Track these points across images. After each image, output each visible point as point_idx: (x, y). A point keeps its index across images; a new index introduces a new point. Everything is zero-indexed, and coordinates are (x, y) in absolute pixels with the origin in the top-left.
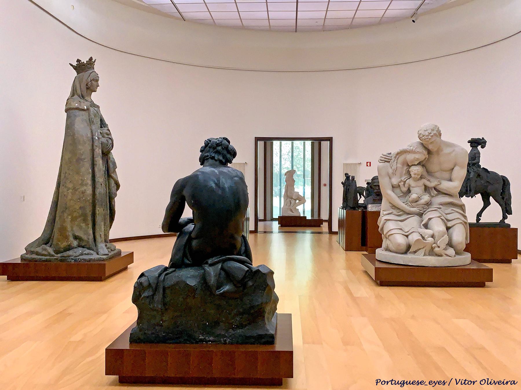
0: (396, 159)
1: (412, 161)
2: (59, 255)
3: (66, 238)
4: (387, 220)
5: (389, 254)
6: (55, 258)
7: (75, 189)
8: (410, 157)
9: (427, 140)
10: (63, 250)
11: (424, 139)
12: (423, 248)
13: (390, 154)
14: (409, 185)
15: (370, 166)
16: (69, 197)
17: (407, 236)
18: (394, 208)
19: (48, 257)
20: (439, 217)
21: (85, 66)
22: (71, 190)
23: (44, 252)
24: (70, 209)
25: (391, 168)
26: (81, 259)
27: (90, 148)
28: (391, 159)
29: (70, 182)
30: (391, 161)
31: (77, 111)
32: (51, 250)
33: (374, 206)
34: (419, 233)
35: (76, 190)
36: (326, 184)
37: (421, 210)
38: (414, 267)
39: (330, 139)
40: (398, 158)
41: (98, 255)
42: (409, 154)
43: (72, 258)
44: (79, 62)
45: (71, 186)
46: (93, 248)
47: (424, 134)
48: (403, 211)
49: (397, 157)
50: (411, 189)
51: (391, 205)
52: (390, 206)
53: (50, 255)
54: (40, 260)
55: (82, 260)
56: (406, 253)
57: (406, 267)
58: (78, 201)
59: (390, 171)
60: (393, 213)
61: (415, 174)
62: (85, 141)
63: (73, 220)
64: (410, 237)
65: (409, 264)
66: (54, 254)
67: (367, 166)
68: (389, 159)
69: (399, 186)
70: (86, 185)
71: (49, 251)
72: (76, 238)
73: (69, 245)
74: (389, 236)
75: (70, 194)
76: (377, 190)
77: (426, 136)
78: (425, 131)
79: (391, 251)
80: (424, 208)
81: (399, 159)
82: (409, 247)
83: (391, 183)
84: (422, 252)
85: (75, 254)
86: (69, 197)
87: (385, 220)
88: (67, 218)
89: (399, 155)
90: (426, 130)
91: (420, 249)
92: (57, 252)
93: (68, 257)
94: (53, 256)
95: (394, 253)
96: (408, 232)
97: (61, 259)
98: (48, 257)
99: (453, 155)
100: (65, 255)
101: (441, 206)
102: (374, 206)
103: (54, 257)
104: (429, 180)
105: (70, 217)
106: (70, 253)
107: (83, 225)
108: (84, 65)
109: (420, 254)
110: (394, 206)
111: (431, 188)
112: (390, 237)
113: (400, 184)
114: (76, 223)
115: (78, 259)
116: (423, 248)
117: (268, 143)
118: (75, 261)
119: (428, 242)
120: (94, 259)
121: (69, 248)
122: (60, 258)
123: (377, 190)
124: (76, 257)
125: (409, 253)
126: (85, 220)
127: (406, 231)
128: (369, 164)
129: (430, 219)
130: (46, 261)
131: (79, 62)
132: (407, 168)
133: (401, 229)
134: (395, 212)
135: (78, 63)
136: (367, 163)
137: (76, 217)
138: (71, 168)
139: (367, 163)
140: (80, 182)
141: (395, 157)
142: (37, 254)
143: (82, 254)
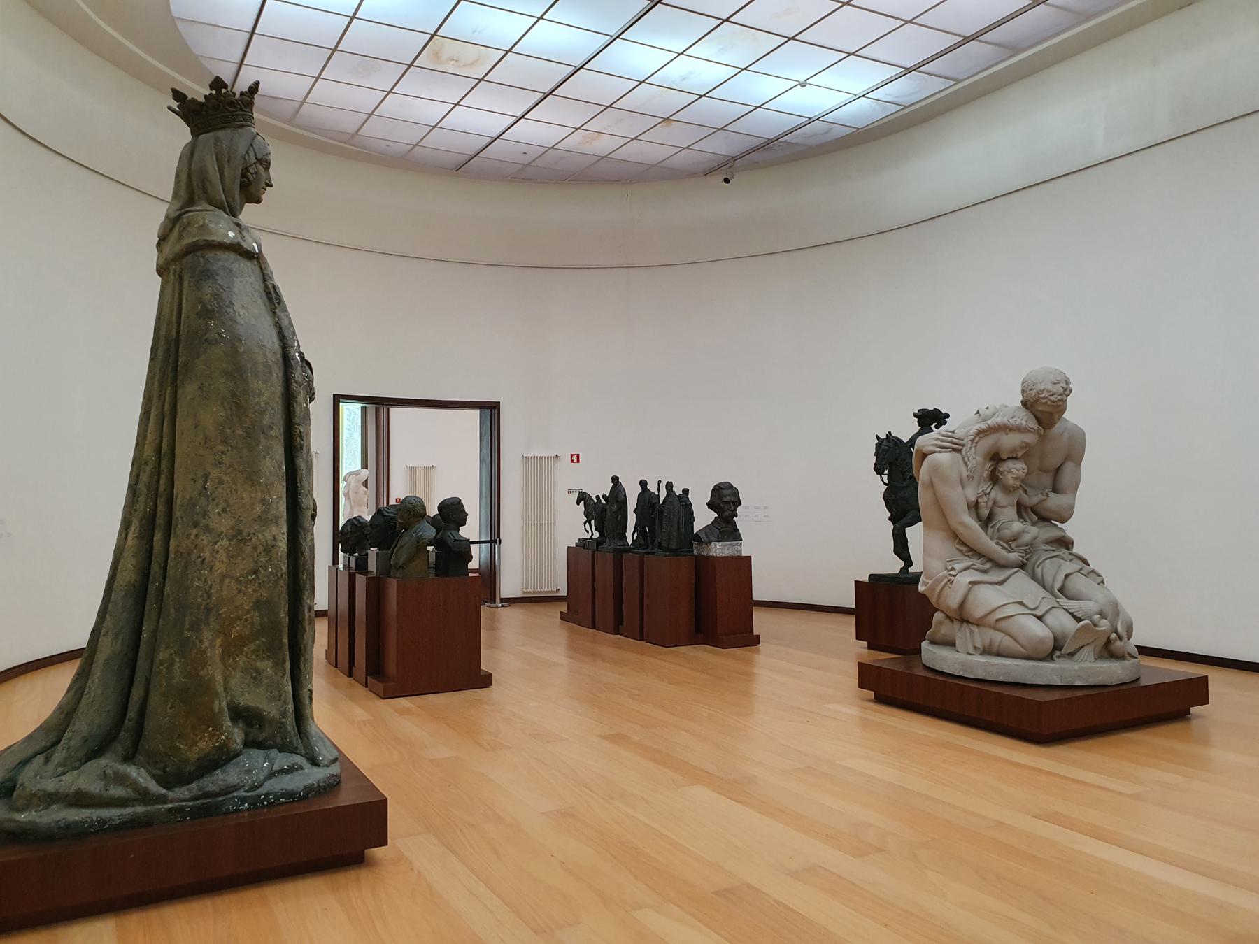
0: (974, 444)
1: (1014, 450)
2: (182, 794)
3: (213, 721)
4: (973, 583)
5: (1017, 663)
6: (170, 806)
7: (239, 537)
8: (1009, 441)
9: (1059, 403)
10: (193, 768)
11: (1053, 402)
12: (1093, 642)
13: (953, 432)
14: (995, 503)
15: (578, 461)
16: (220, 567)
17: (1040, 618)
18: (970, 554)
19: (140, 809)
20: (1079, 571)
21: (235, 107)
22: (225, 542)
23: (117, 791)
24: (220, 612)
25: (966, 463)
26: (275, 794)
27: (279, 389)
28: (963, 445)
29: (224, 510)
30: (964, 449)
31: (233, 256)
32: (140, 775)
33: (726, 545)
34: (1066, 610)
35: (243, 541)
36: (396, 499)
37: (1022, 557)
38: (961, 683)
39: (491, 410)
40: (978, 441)
41: (315, 769)
42: (1007, 434)
43: (241, 793)
44: (219, 91)
45: (224, 525)
46: (296, 745)
47: (1055, 391)
48: (989, 560)
49: (976, 440)
50: (997, 510)
51: (964, 549)
52: (961, 551)
53: (144, 796)
54: (104, 828)
55: (282, 796)
56: (1049, 657)
57: (1096, 692)
58: (251, 581)
59: (965, 473)
60: (974, 567)
61: (1015, 479)
62: (271, 363)
63: (231, 650)
64: (1048, 618)
65: (1076, 684)
66: (164, 791)
67: (572, 461)
68: (960, 445)
69: (977, 503)
70: (276, 521)
71: (141, 780)
72: (241, 715)
73: (221, 748)
74: (997, 620)
75: (222, 555)
76: (731, 511)
77: (1059, 395)
78: (1055, 384)
79: (998, 655)
80: (1027, 553)
81: (978, 444)
82: (1058, 645)
83: (966, 498)
84: (1087, 654)
85: (248, 780)
86: (220, 567)
87: (970, 583)
88: (212, 646)
89: (981, 435)
90: (1056, 382)
91: (1083, 647)
92: (169, 781)
93: (223, 795)
94: (162, 799)
95: (1016, 660)
96: (1036, 609)
97: (200, 807)
98: (140, 809)
99: (1066, 434)
100: (212, 788)
101: (1047, 547)
102: (726, 545)
103: (166, 803)
104: (1026, 492)
105: (219, 641)
106: (230, 775)
107: (266, 666)
108: (232, 104)
109: (1086, 657)
110: (972, 550)
111: (1026, 508)
112: (1003, 624)
113: (980, 500)
114: (241, 660)
115: (267, 795)
116: (1093, 642)
117: (382, 410)
118: (255, 805)
119: (1104, 628)
120: (319, 785)
121: (221, 758)
122: (191, 804)
123: (731, 511)
124: (258, 788)
125: (1058, 657)
126: (271, 650)
127: (1032, 607)
128: (575, 458)
129: (1067, 576)
130: (134, 824)
131: (219, 91)
132: (991, 465)
133: (1021, 603)
134: (977, 563)
135: (214, 92)
136: (572, 455)
137: (240, 637)
138: (226, 459)
139: (572, 455)
140: (258, 510)
141: (972, 441)
142: (80, 799)
143: (271, 775)
